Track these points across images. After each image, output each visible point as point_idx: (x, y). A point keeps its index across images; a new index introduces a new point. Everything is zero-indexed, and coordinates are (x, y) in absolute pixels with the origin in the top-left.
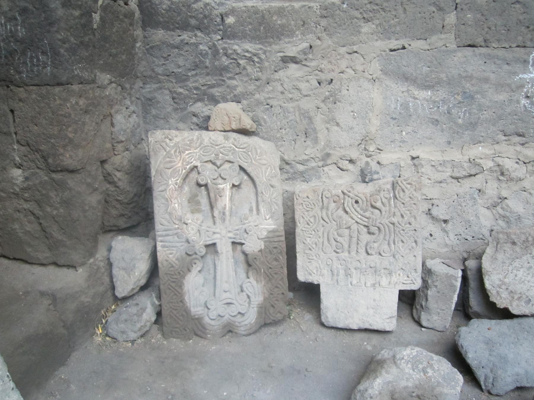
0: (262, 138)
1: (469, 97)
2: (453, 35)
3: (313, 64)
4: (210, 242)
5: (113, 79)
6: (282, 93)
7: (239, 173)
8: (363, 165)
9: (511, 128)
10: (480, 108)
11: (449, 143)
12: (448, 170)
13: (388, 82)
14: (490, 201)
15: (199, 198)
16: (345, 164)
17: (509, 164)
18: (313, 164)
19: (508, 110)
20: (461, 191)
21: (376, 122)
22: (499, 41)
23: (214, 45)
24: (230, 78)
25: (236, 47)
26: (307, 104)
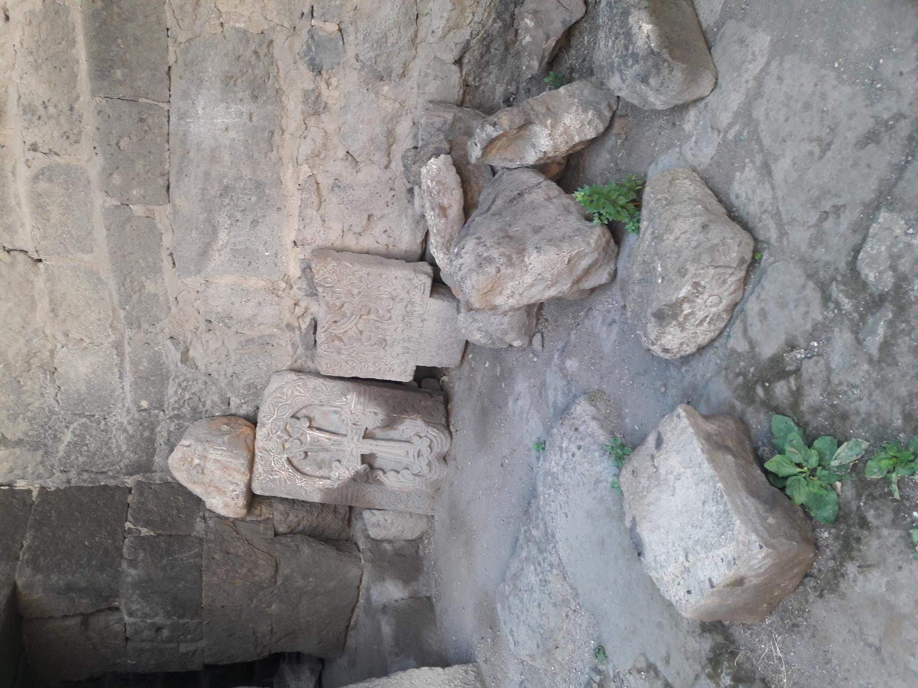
0: (268, 382)
1: (226, 190)
2: (156, 207)
3: (189, 336)
4: (359, 459)
5: (201, 514)
6: (220, 363)
7: (298, 418)
10: (239, 178)
11: (279, 209)
12: (310, 212)
13: (209, 270)
14: (349, 170)
15: (319, 459)
16: (299, 311)
17: (306, 148)
18: (298, 339)
19: (242, 149)
20: (335, 200)
21: (254, 282)
22: (162, 163)
23: (170, 418)
24: (204, 406)
25: (172, 401)
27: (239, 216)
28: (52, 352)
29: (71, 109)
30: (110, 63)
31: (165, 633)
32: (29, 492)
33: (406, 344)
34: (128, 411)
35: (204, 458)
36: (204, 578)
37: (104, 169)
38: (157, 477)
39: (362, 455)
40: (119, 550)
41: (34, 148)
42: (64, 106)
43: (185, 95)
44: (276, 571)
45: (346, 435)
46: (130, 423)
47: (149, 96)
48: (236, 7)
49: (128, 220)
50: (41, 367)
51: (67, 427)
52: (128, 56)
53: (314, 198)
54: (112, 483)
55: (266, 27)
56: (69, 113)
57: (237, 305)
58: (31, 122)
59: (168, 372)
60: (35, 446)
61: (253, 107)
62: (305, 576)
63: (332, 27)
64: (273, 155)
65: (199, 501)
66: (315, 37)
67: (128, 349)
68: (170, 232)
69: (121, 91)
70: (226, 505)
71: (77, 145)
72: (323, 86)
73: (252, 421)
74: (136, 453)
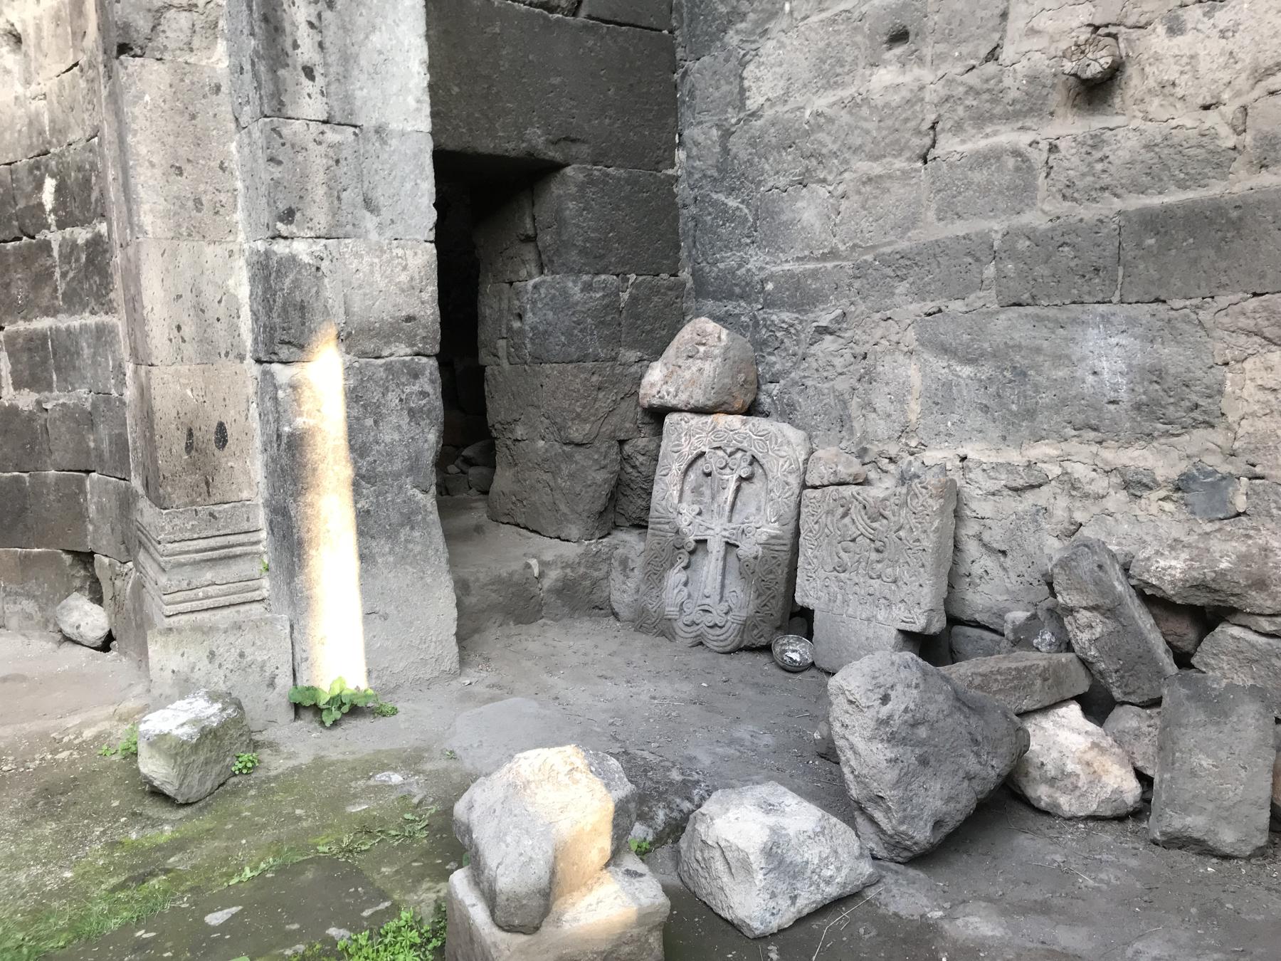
3: (848, 334)
7: (751, 464)
8: (904, 467)
9: (1080, 418)
11: (1004, 438)
12: (1003, 477)
13: (925, 356)
14: (1059, 526)
15: (703, 489)
17: (1080, 471)
19: (1073, 393)
21: (914, 408)
22: (1049, 296)
23: (755, 316)
24: (770, 354)
25: (774, 317)
26: (842, 385)
27: (992, 390)
28: (824, 181)
29: (1103, 189)
30: (1163, 230)
31: (516, 324)
32: (673, 165)
33: (839, 597)
34: (761, 269)
35: (706, 357)
36: (570, 366)
37: (1034, 230)
38: (691, 304)
39: (705, 541)
40: (605, 271)
41: (1053, 149)
42: (1106, 180)
43: (1132, 321)
44: (578, 445)
45: (730, 521)
46: (749, 270)
47: (1128, 279)
48: (1252, 380)
49: (977, 260)
50: (807, 170)
51: (742, 202)
52: (1173, 252)
53: (1020, 482)
54: (683, 254)
55: (1230, 419)
56: (1098, 186)
57: (886, 390)
58: (1083, 144)
59: (806, 312)
60: (723, 168)
61: (1125, 405)
62: (572, 476)
63: (1241, 503)
64: (1070, 431)
65: (657, 354)
66: (1224, 483)
67: (829, 265)
68: (965, 309)
69: (1129, 246)
70: (652, 385)
71: (1059, 197)
72: (1163, 493)
73: (751, 410)
74: (716, 279)
